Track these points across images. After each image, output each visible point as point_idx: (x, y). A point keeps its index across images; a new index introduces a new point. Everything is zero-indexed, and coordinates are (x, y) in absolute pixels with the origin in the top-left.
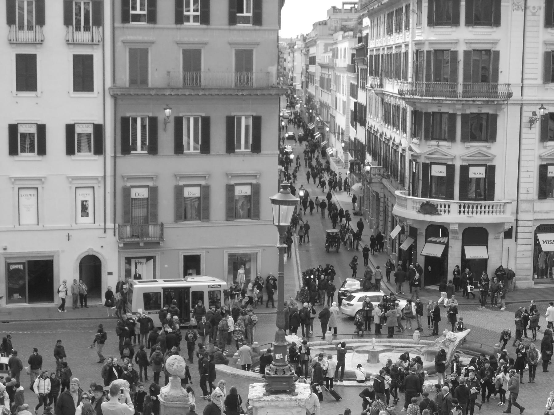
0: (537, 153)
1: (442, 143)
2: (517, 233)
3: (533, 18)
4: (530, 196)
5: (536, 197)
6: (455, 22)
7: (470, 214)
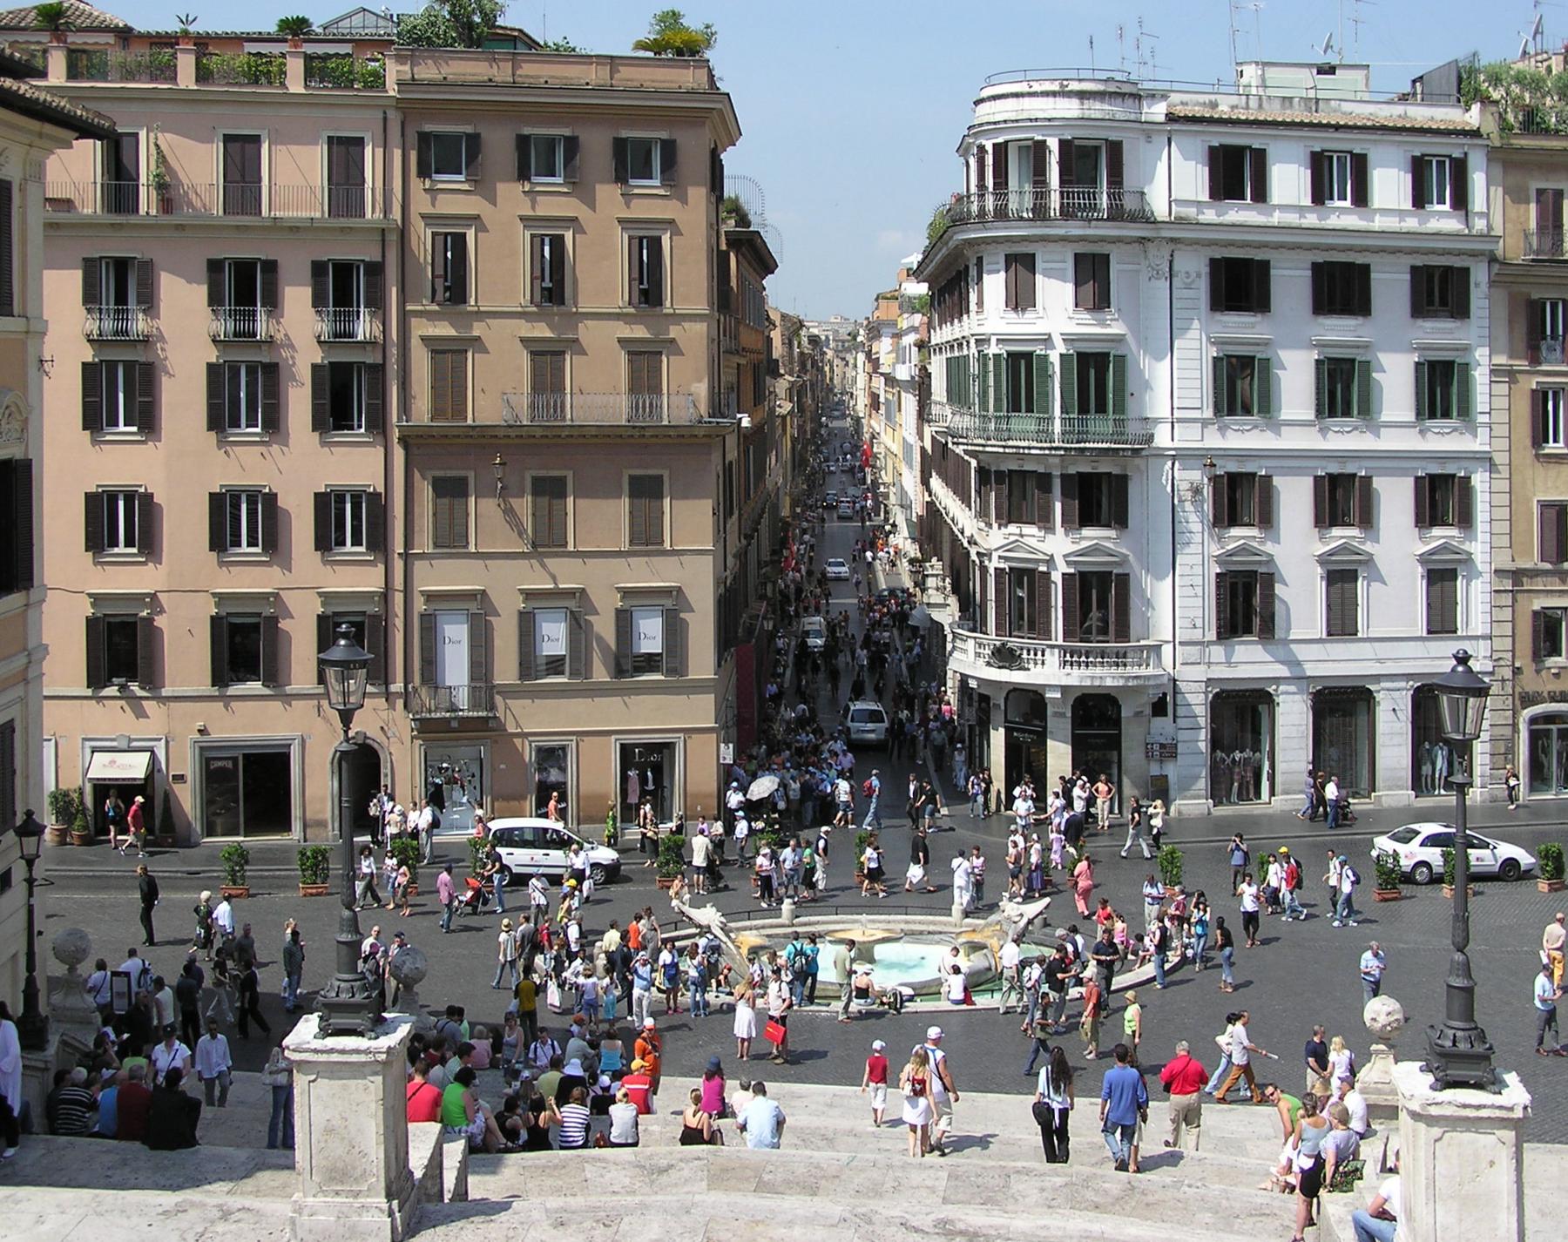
2: (1175, 704)
3: (1186, 293)
4: (1197, 635)
7: (1039, 666)
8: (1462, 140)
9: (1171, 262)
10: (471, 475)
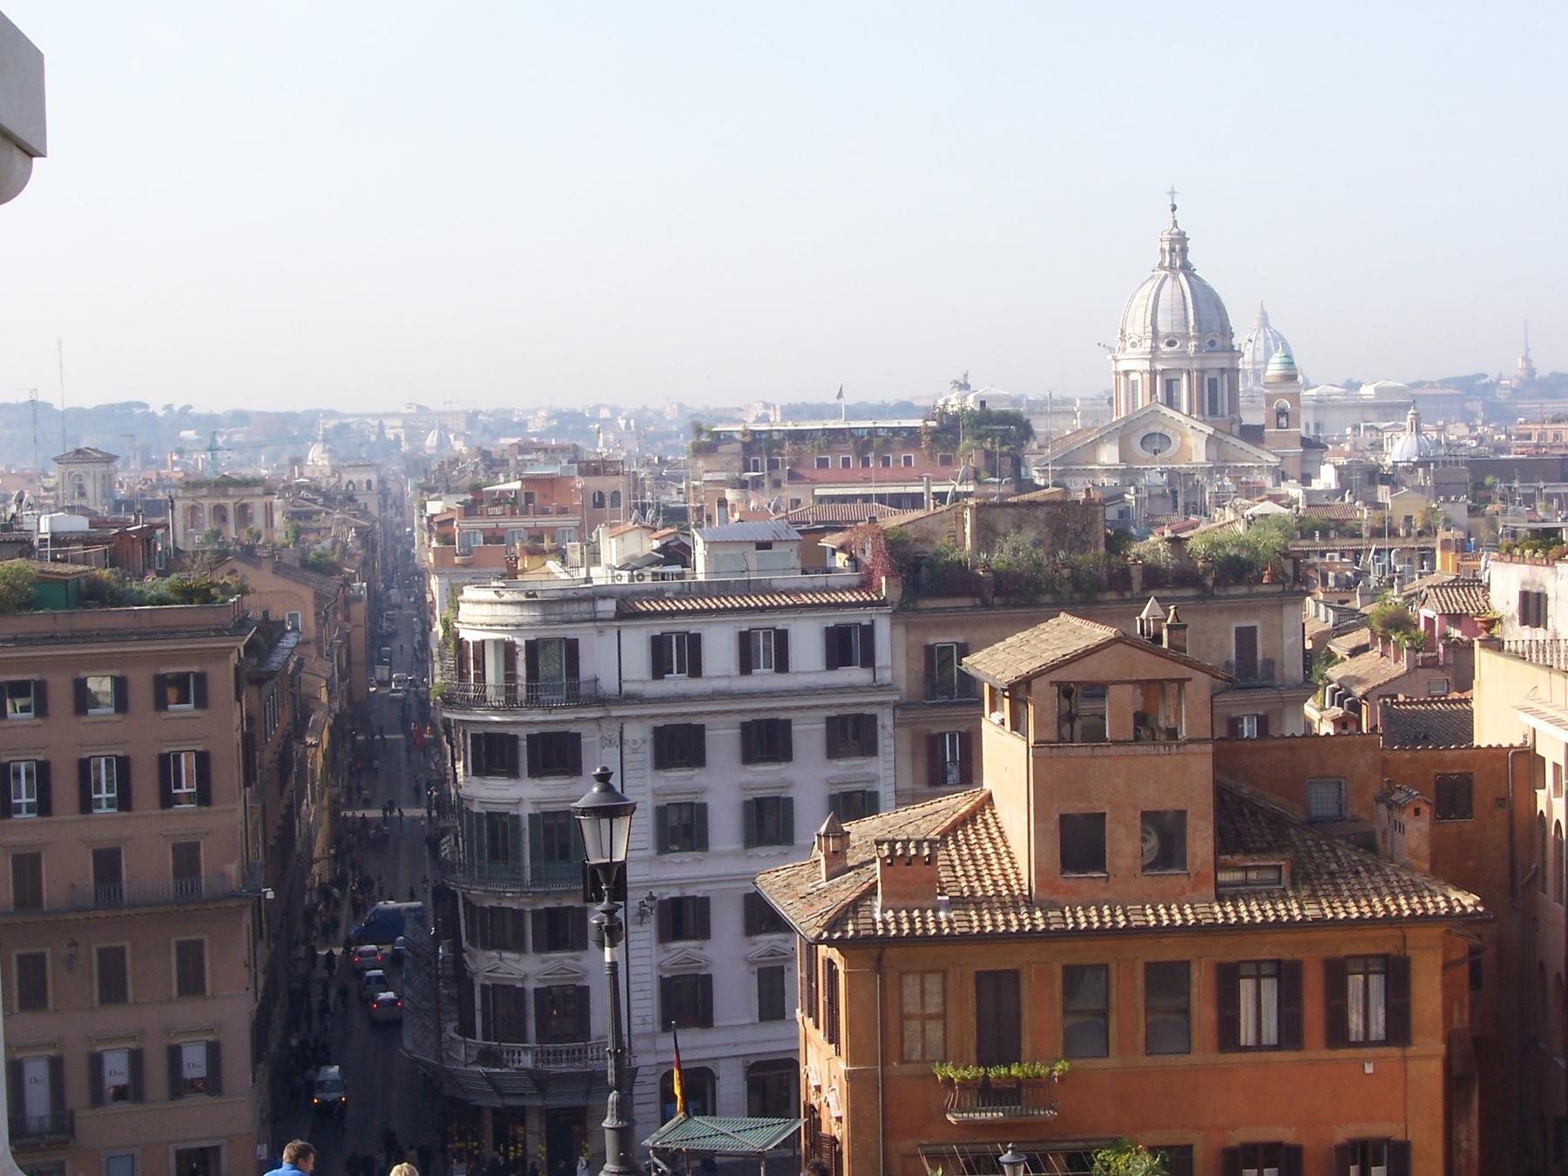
0: (655, 962)
1: (506, 955)
3: (634, 757)
4: (649, 1028)
5: (658, 1028)
6: (512, 772)
8: (869, 610)
9: (621, 733)
10: (48, 951)
